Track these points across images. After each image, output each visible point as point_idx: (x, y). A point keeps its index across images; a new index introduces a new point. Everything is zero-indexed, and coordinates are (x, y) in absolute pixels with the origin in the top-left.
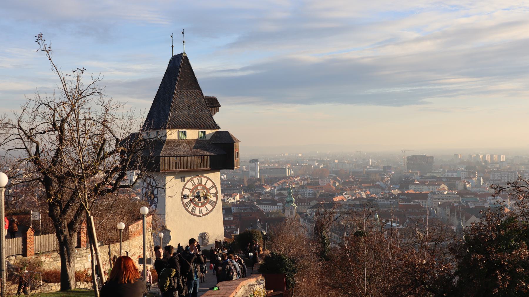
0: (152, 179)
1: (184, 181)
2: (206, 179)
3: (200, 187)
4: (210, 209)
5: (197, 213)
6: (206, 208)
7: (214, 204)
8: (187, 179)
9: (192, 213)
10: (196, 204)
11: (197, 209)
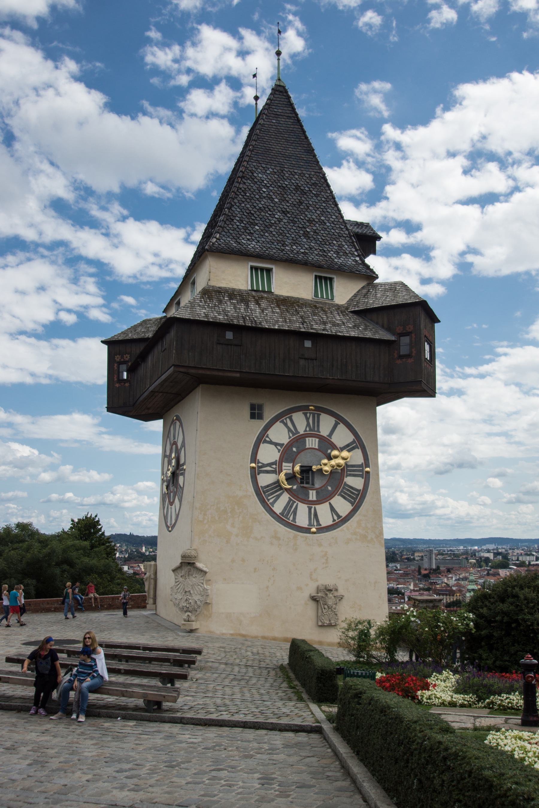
0: (178, 423)
1: (260, 417)
2: (332, 421)
3: (312, 443)
4: (343, 514)
5: (302, 519)
6: (332, 509)
7: (357, 498)
8: (269, 414)
9: (285, 519)
10: (300, 496)
11: (302, 509)
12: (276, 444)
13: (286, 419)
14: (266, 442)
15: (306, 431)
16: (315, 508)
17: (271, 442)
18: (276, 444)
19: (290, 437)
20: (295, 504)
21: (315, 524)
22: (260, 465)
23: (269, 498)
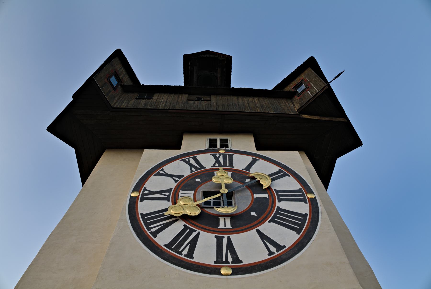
12: (172, 176)
13: (188, 159)
14: (159, 174)
15: (214, 165)
16: (229, 238)
17: (166, 175)
18: (172, 176)
19: (192, 171)
20: (194, 234)
21: (230, 259)
22: (146, 192)
23: (150, 227)
